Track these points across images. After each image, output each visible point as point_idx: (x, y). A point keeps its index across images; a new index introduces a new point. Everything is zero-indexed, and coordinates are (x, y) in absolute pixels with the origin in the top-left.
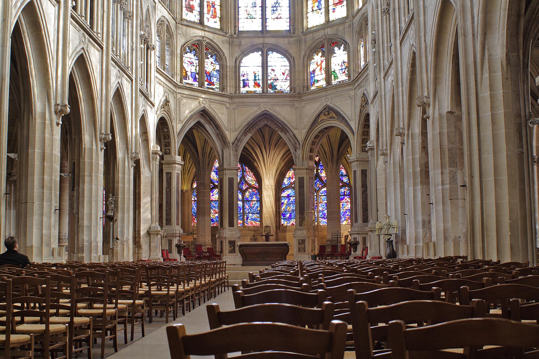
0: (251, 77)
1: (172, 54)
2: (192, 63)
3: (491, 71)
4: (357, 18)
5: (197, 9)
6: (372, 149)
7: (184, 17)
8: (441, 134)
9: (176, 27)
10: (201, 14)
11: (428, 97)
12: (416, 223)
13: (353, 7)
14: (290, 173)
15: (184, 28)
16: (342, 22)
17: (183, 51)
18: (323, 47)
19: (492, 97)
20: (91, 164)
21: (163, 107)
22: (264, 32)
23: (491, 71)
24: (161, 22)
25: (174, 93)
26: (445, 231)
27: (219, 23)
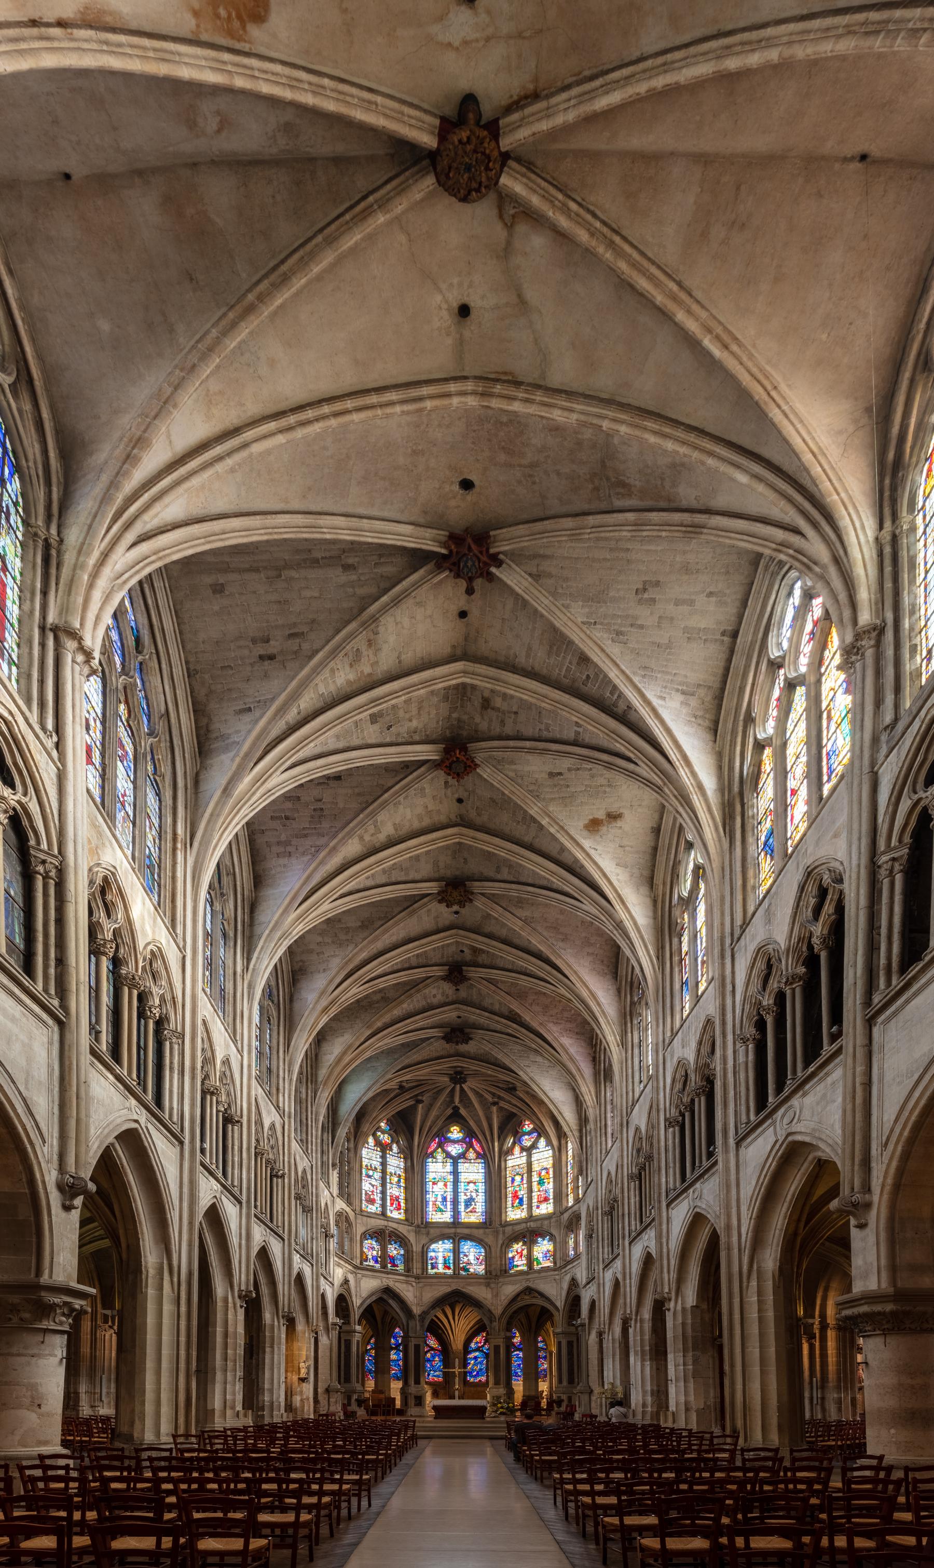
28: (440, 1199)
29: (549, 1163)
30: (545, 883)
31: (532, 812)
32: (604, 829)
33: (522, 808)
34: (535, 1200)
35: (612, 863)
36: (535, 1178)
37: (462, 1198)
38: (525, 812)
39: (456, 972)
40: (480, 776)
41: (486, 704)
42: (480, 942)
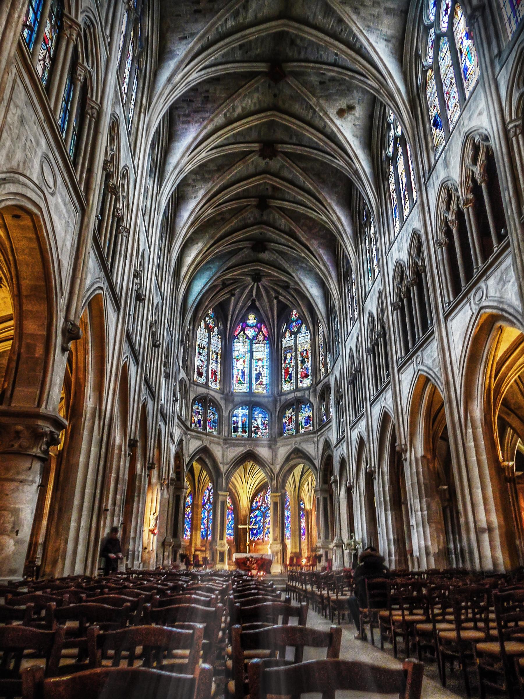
0: (240, 425)
1: (186, 405)
2: (199, 412)
3: (474, 428)
4: (319, 387)
5: (205, 375)
6: (335, 481)
7: (195, 379)
8: (418, 473)
9: (190, 386)
10: (207, 377)
11: (406, 445)
12: (389, 540)
13: (316, 377)
14: (258, 498)
15: (195, 387)
16: (308, 388)
17: (193, 403)
18: (293, 405)
19: (476, 446)
20: (140, 487)
21: (179, 444)
22: (251, 393)
23: (474, 428)
24: (181, 381)
25: (186, 434)
26: (426, 548)
27: (219, 385)
28: (240, 374)
29: (307, 346)
30: (315, 145)
31: (311, 103)
32: (346, 115)
33: (305, 100)
34: (299, 376)
35: (348, 131)
36: (300, 358)
37: (254, 373)
38: (308, 103)
39: (263, 201)
40: (286, 81)
41: (293, 43)
42: (277, 182)
